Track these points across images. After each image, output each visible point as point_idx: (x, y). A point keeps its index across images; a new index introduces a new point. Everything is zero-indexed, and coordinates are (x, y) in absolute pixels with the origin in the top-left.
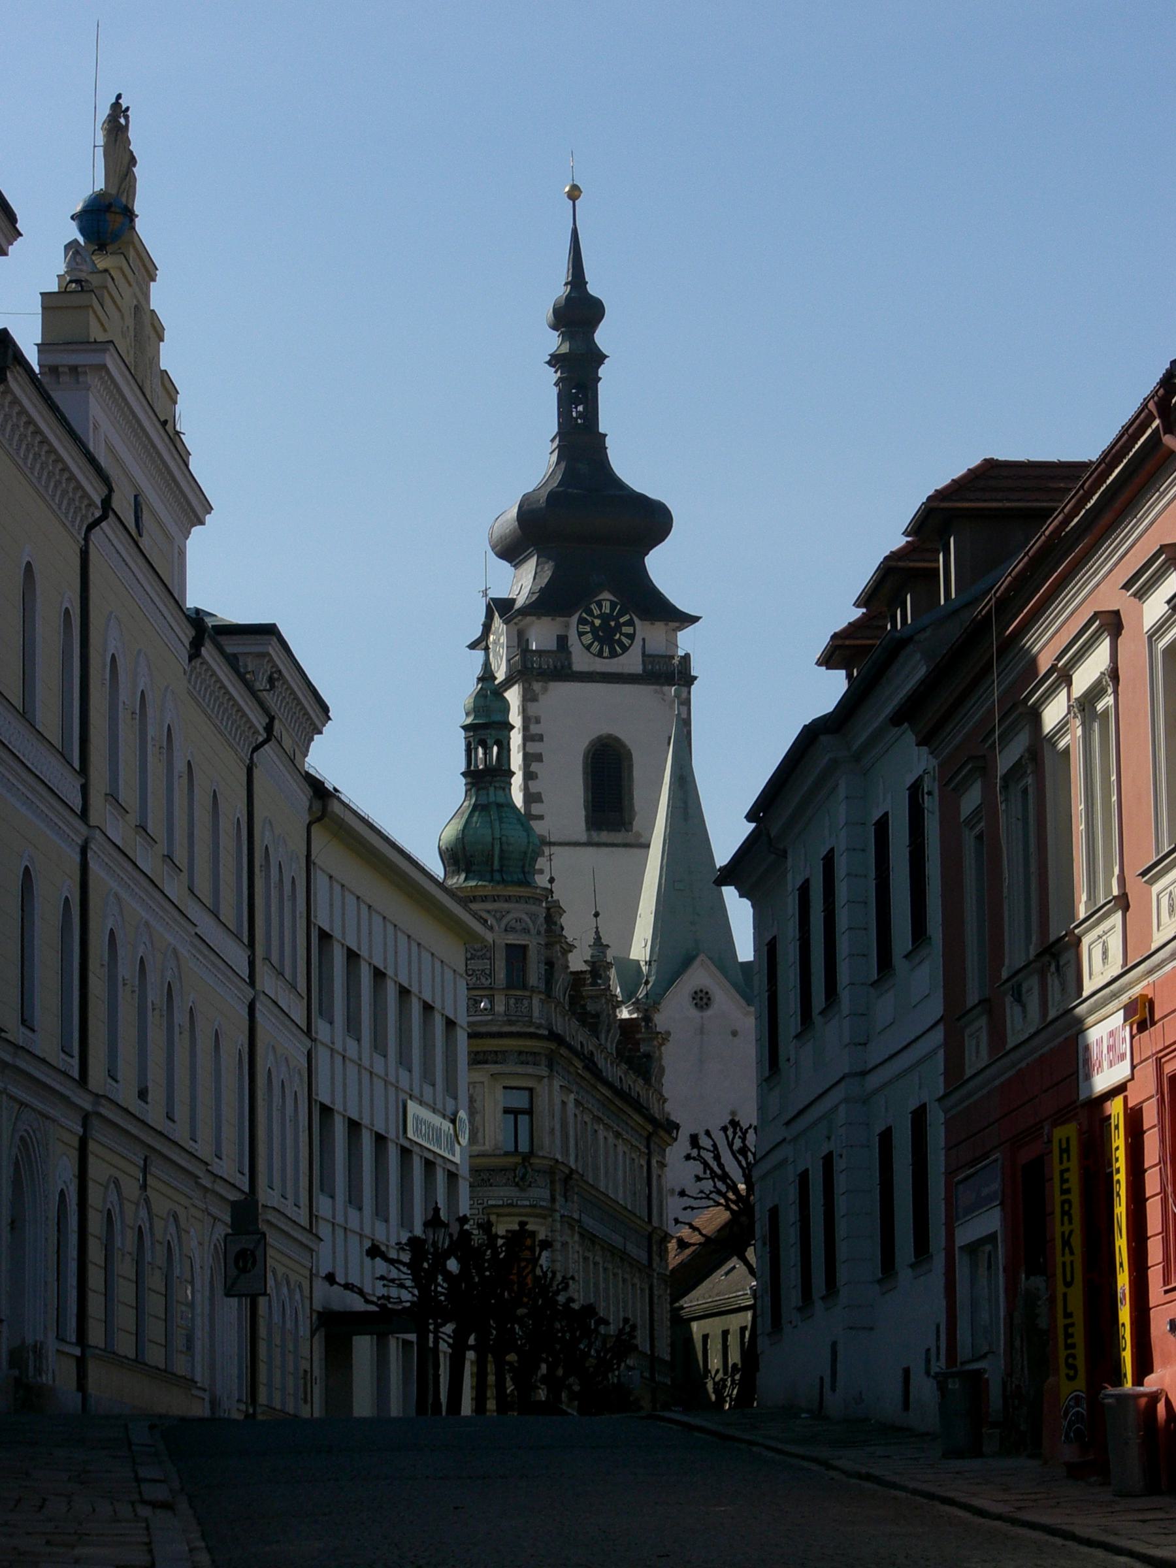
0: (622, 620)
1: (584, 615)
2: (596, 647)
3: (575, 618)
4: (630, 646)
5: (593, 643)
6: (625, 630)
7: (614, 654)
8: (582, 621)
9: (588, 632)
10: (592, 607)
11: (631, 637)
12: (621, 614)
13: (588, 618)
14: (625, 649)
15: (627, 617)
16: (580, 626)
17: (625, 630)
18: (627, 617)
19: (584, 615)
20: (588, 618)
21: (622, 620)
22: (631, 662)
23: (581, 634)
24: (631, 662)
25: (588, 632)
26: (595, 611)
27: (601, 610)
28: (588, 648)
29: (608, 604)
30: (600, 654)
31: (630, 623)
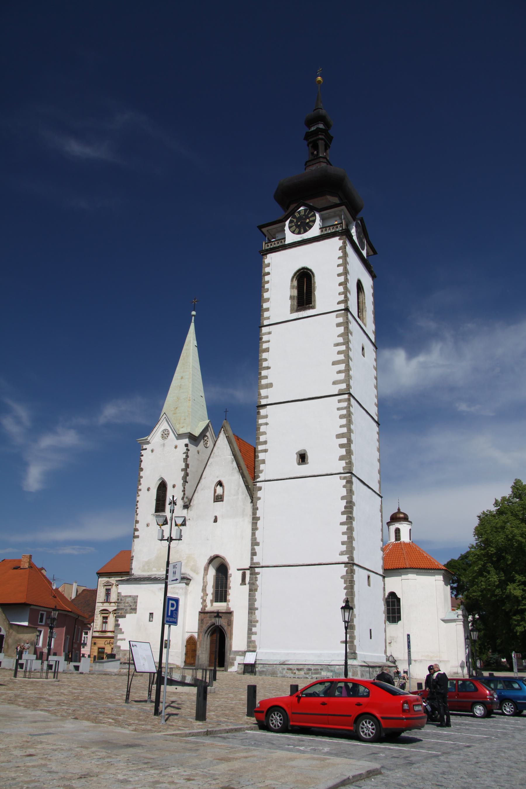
1: (292, 219)
2: (297, 230)
3: (287, 223)
4: (313, 225)
5: (296, 229)
7: (305, 231)
8: (290, 223)
9: (294, 226)
11: (314, 221)
12: (309, 213)
14: (310, 227)
19: (292, 219)
22: (315, 231)
25: (294, 226)
26: (297, 216)
27: (299, 214)
28: (293, 232)
30: (299, 233)
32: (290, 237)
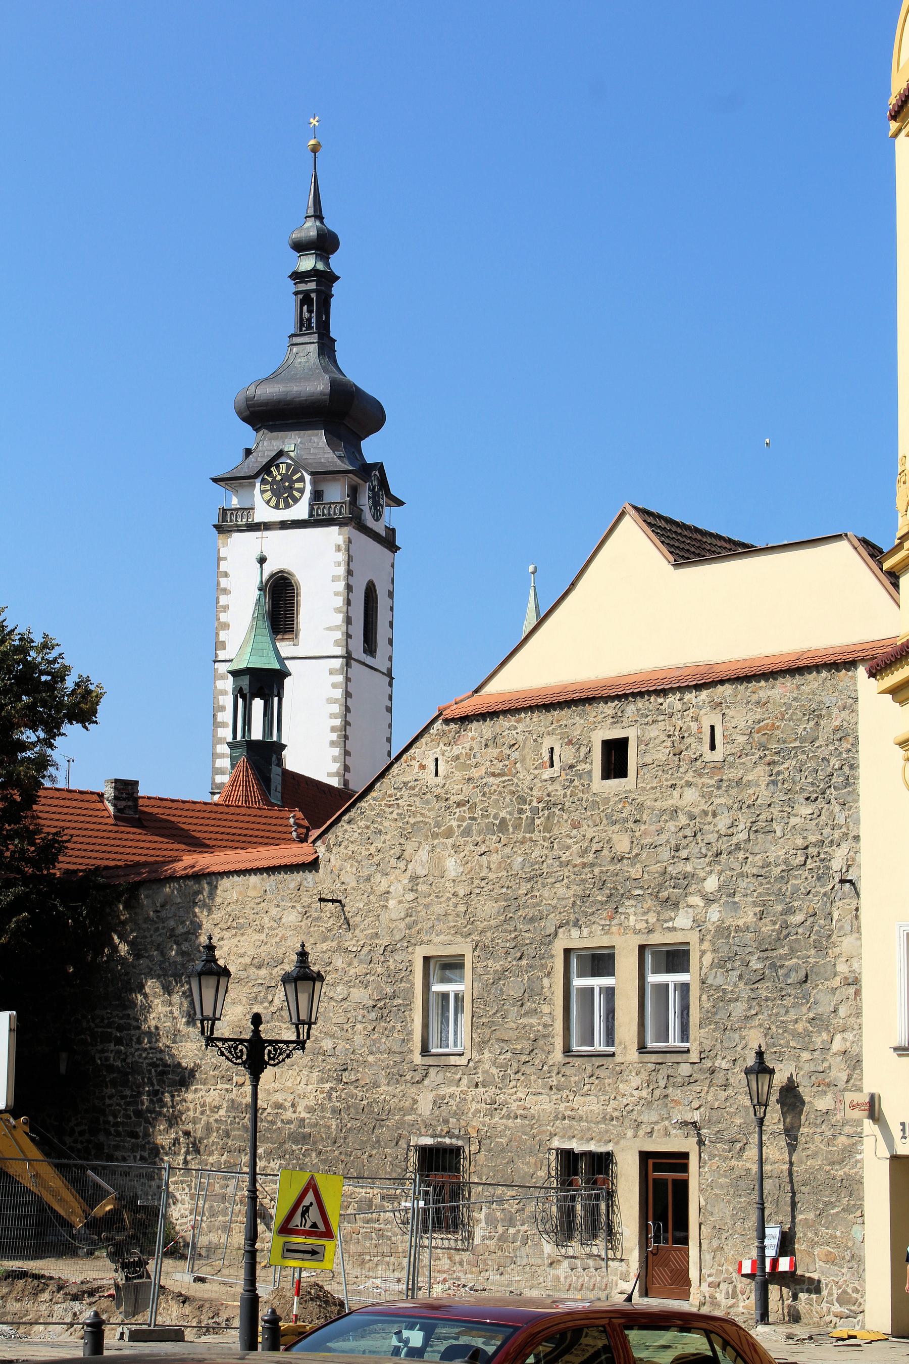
0: (294, 478)
2: (273, 502)
4: (300, 498)
6: (297, 485)
7: (287, 506)
9: (268, 490)
10: (272, 469)
11: (302, 491)
13: (269, 479)
14: (296, 500)
15: (299, 475)
16: (263, 486)
17: (297, 485)
18: (299, 475)
19: (266, 476)
20: (269, 479)
21: (294, 478)
22: (300, 510)
23: (263, 492)
24: (300, 510)
25: (268, 490)
28: (268, 502)
29: (284, 465)
30: (277, 507)
31: (302, 479)
32: (263, 512)
